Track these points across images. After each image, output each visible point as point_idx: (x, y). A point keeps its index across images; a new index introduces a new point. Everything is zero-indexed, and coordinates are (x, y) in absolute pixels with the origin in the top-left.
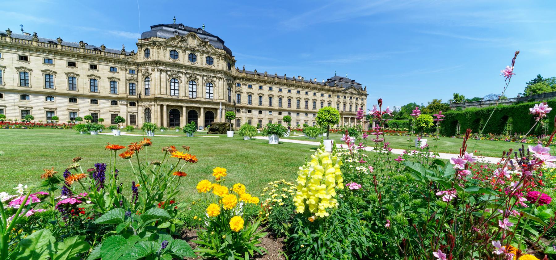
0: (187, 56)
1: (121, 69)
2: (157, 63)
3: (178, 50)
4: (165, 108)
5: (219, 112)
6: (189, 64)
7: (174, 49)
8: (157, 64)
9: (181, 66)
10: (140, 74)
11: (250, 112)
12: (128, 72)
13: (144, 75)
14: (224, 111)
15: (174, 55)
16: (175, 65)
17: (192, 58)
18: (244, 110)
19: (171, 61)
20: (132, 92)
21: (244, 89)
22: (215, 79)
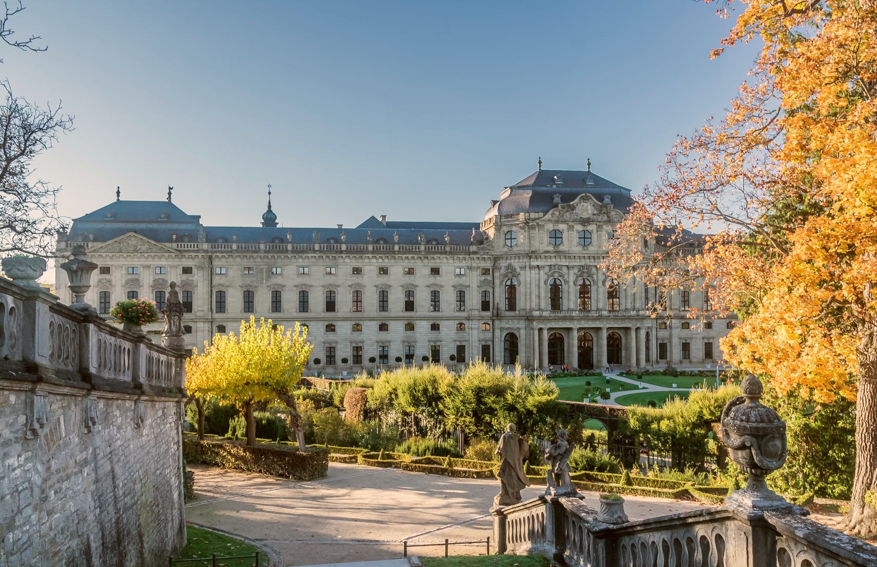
0: (575, 236)
1: (470, 268)
2: (531, 254)
3: (562, 227)
4: (545, 332)
5: (633, 333)
7: (556, 228)
8: (530, 257)
10: (497, 274)
12: (479, 272)
13: (506, 276)
14: (643, 333)
15: (556, 236)
16: (558, 253)
17: (585, 239)
19: (551, 248)
20: (485, 306)
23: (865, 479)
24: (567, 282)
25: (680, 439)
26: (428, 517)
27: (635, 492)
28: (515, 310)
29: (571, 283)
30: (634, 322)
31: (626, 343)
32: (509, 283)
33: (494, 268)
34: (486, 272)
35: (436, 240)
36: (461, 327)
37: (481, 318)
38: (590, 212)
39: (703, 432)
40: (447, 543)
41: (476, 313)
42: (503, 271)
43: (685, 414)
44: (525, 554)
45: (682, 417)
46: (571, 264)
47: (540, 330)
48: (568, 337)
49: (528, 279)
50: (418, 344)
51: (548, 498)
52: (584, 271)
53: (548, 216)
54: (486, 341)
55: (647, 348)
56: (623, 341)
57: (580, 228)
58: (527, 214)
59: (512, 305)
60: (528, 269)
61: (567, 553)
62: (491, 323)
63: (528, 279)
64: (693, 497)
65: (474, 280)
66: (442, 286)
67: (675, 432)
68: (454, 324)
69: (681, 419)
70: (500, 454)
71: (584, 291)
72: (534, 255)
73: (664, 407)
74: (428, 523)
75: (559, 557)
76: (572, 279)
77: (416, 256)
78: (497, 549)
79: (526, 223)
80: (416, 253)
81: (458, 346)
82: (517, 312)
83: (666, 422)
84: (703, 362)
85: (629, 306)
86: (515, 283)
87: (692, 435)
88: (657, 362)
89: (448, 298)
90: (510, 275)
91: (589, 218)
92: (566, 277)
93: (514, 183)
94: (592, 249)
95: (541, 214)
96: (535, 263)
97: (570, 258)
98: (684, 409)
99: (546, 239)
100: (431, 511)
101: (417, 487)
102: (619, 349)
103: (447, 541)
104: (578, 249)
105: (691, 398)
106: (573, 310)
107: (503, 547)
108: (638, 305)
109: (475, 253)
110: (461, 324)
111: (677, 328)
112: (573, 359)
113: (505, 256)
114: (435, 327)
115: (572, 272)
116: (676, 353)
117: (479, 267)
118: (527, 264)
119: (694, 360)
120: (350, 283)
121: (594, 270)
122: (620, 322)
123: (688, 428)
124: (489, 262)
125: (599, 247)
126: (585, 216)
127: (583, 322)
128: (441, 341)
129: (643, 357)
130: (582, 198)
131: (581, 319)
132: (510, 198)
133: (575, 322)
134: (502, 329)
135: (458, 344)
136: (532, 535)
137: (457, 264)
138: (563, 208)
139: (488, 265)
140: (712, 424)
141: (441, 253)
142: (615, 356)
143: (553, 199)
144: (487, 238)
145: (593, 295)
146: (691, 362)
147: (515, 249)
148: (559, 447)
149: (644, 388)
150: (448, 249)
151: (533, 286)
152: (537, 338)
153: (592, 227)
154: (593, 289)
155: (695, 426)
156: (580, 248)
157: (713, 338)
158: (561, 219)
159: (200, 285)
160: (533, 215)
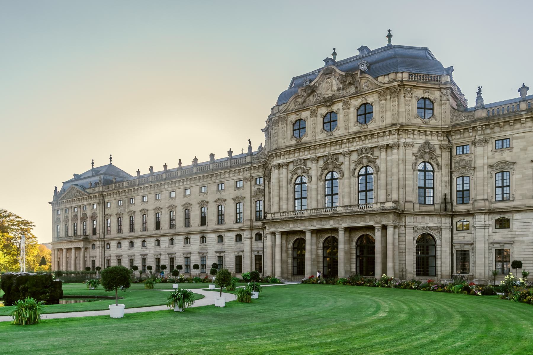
6: (322, 136)
9: (308, 147)
11: (503, 224)
16: (299, 147)
18: (480, 220)
19: (294, 142)
21: (483, 156)
22: (376, 153)
24: (310, 178)
29: (314, 179)
37: (252, 229)
92: (310, 171)
94: (338, 133)
99: (289, 133)
117: (252, 178)
120: (168, 205)
121: (341, 159)
122: (358, 219)
125: (346, 129)
127: (315, 223)
133: (307, 223)
159: (98, 215)
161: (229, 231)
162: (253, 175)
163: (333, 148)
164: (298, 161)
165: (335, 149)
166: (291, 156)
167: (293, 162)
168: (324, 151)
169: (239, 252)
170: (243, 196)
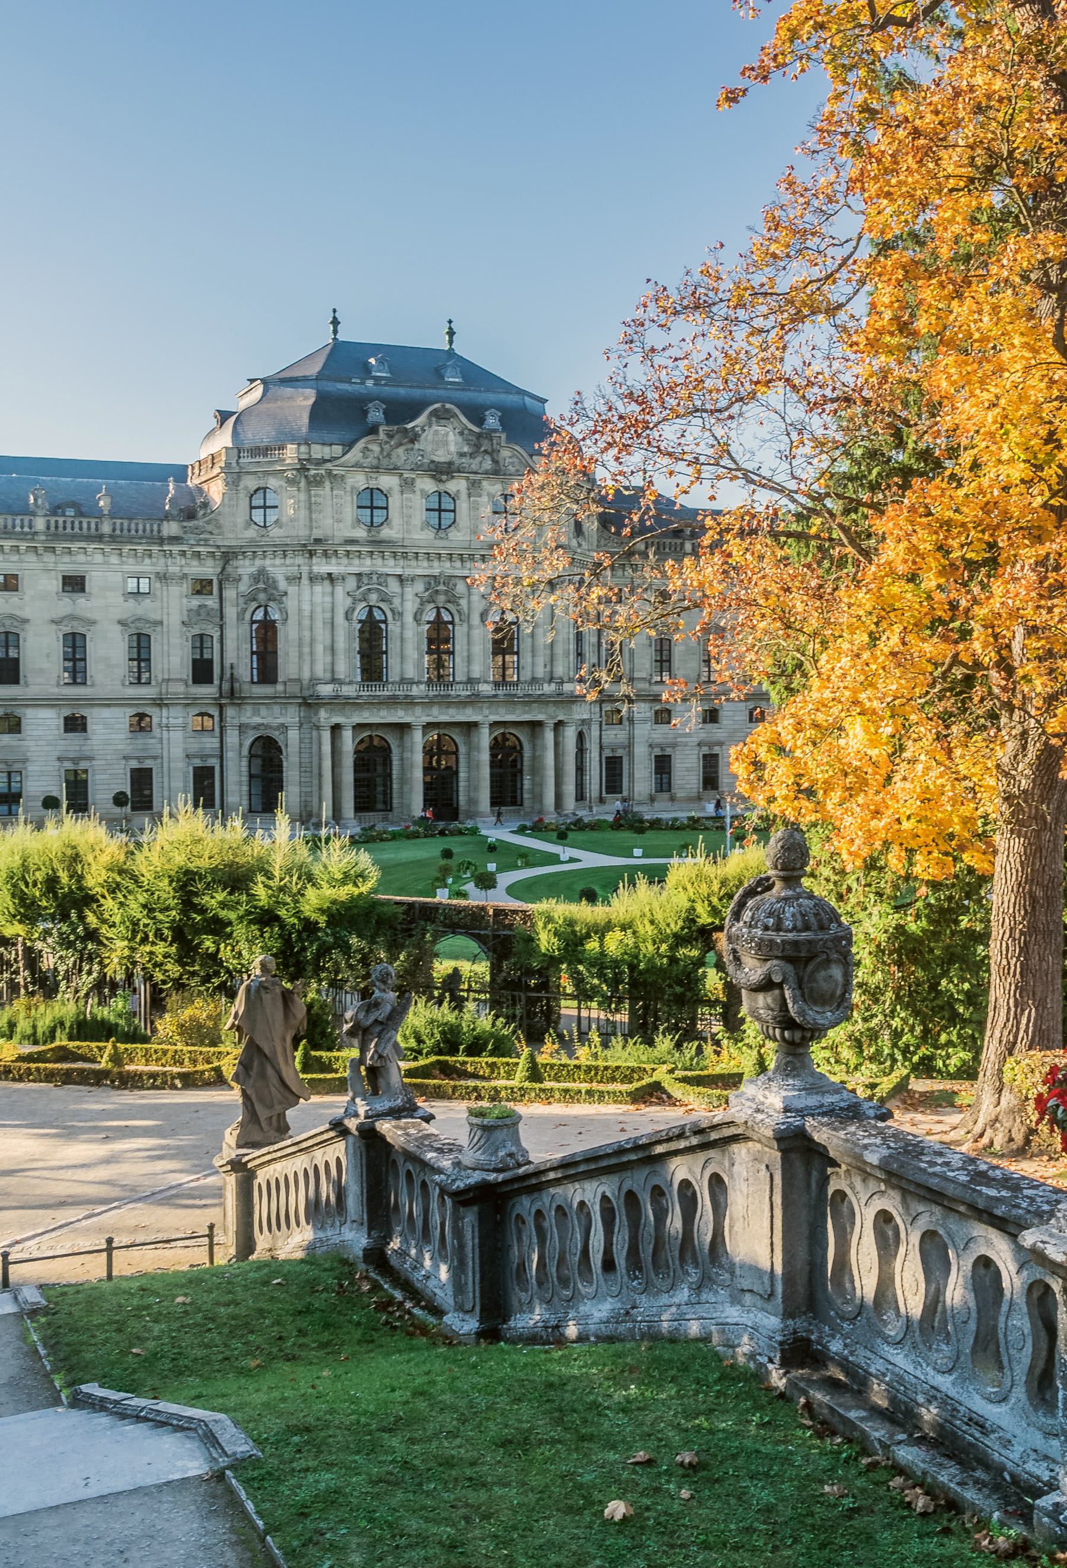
0: (418, 504)
1: (163, 578)
2: (314, 547)
3: (387, 482)
4: (347, 735)
5: (549, 736)
7: (373, 484)
8: (312, 554)
9: (399, 551)
10: (230, 594)
12: (186, 587)
17: (441, 512)
19: (361, 533)
20: (202, 671)
23: (1006, 1033)
24: (398, 615)
25: (647, 971)
26: (62, 1190)
27: (547, 1096)
28: (274, 681)
29: (409, 618)
30: (551, 709)
31: (534, 758)
32: (259, 615)
33: (224, 578)
34: (202, 587)
35: (74, 505)
36: (141, 724)
37: (190, 702)
38: (452, 448)
39: (695, 953)
40: (110, 1247)
41: (180, 688)
42: (244, 587)
43: (659, 916)
44: (299, 1255)
45: (652, 922)
46: (408, 572)
47: (336, 729)
48: (402, 746)
49: (306, 607)
50: (31, 768)
51: (352, 1124)
52: (440, 590)
53: (355, 454)
54: (204, 757)
55: (580, 769)
56: (527, 754)
57: (427, 485)
58: (303, 448)
59: (267, 668)
60: (305, 581)
61: (395, 1244)
62: (216, 714)
63: (306, 607)
64: (670, 1097)
65: (173, 606)
66: (93, 623)
67: (636, 956)
68: (123, 717)
69: (649, 928)
70: (239, 1029)
71: (439, 639)
72: (319, 549)
73: (615, 901)
74: (62, 1204)
75: (376, 1257)
76: (410, 607)
77: (23, 545)
78: (233, 1251)
79: (302, 469)
80: (22, 536)
81: (133, 771)
82: (280, 687)
83: (618, 934)
84: (699, 798)
85: (540, 672)
86: (275, 616)
87: (673, 960)
88: (602, 800)
89: (108, 653)
90: (262, 597)
91: (450, 464)
92: (397, 602)
93: (270, 370)
94: (458, 537)
95: (338, 450)
96: (322, 567)
97: (405, 556)
98: (656, 905)
99: (349, 511)
100: (68, 1174)
101: (34, 1120)
102: (517, 772)
103: (110, 1241)
104: (423, 537)
105: (672, 879)
106: (412, 682)
107: (246, 1245)
108: (560, 670)
109: (175, 540)
110: (141, 716)
111: (645, 721)
112: (414, 801)
113: (253, 550)
114: (75, 724)
115: (410, 592)
116: (641, 778)
117: (185, 576)
118: (305, 569)
119: (681, 795)
121: (461, 588)
122: (519, 709)
123: (664, 947)
124: (210, 562)
126: (441, 457)
127: (435, 710)
128: (90, 758)
129: (570, 788)
130: (435, 414)
131: (430, 703)
132: (263, 407)
133: (418, 710)
134: (242, 728)
135: (134, 764)
136: (315, 1211)
137: (131, 566)
138: (390, 436)
139: (209, 569)
140: (715, 936)
141: (89, 538)
142: (507, 791)
143: (365, 413)
144: (205, 505)
145: (460, 645)
146: (672, 799)
147: (275, 532)
148: (377, 1005)
149: (572, 860)
150: (106, 528)
151: (319, 624)
152: (327, 748)
153: (457, 485)
154: (460, 631)
155: (679, 940)
156: (428, 535)
157: (721, 744)
158: (385, 462)
160: (318, 451)
161: (108, 705)
162: (186, 570)
163: (448, 564)
164: (375, 577)
165: (454, 568)
166: (356, 561)
167: (359, 575)
168: (431, 567)
169: (146, 758)
170: (158, 618)
